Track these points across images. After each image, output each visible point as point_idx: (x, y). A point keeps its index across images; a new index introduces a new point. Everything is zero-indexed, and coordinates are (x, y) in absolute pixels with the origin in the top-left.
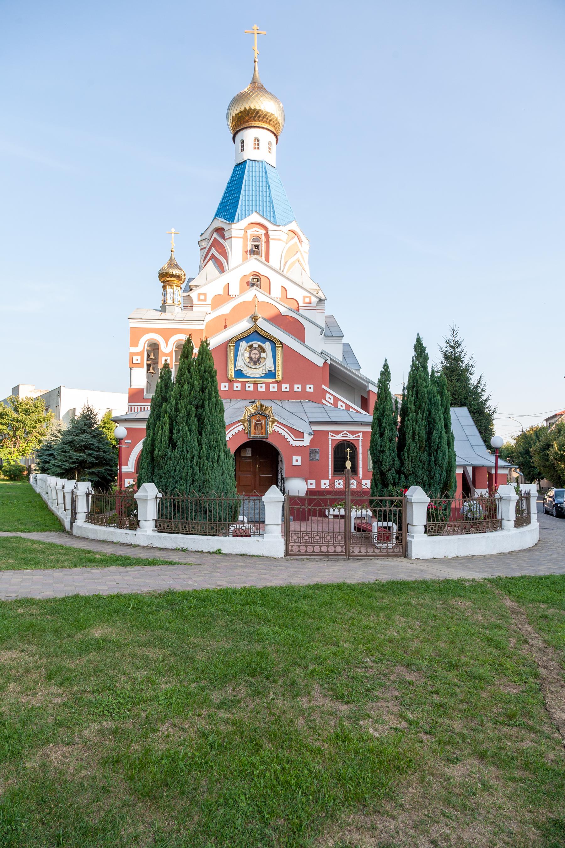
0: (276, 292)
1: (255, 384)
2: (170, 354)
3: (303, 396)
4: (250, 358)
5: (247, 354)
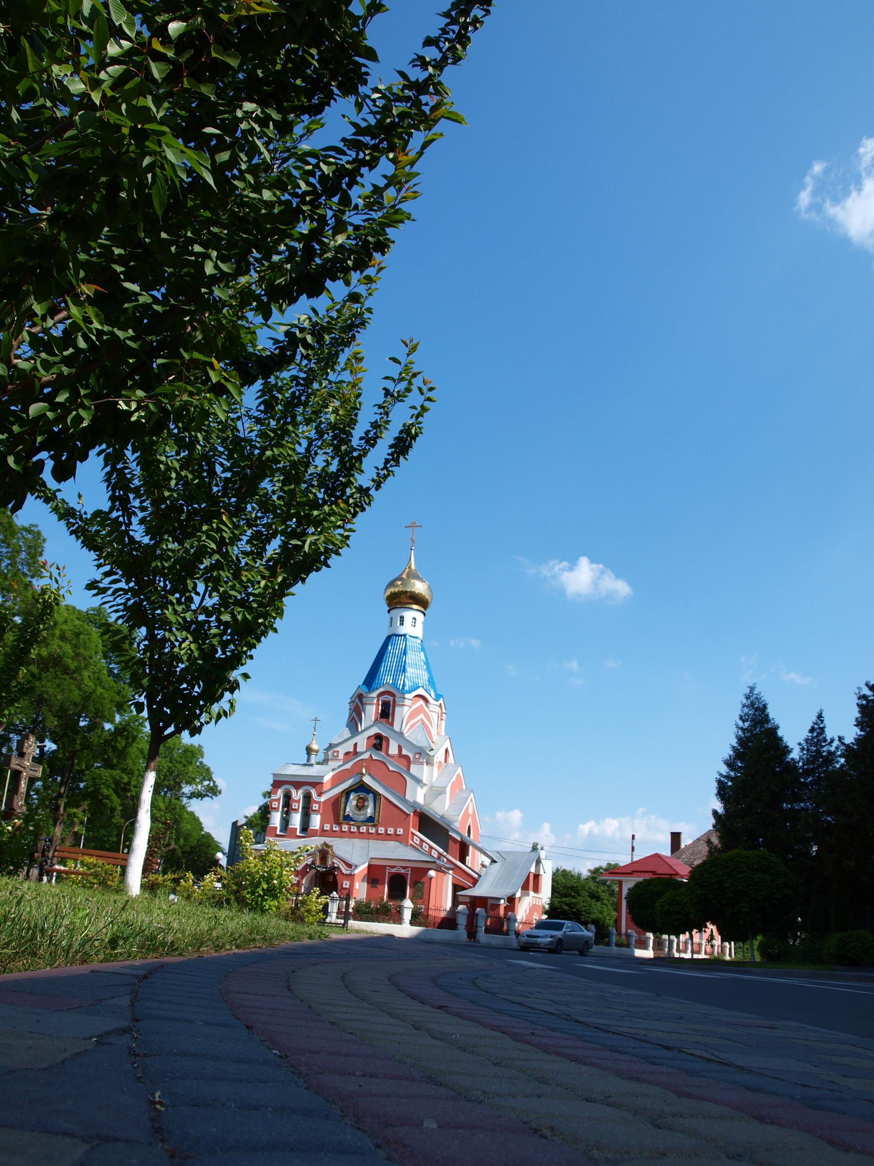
0: (393, 750)
1: (358, 828)
2: (298, 801)
3: (396, 837)
4: (357, 805)
5: (355, 802)
